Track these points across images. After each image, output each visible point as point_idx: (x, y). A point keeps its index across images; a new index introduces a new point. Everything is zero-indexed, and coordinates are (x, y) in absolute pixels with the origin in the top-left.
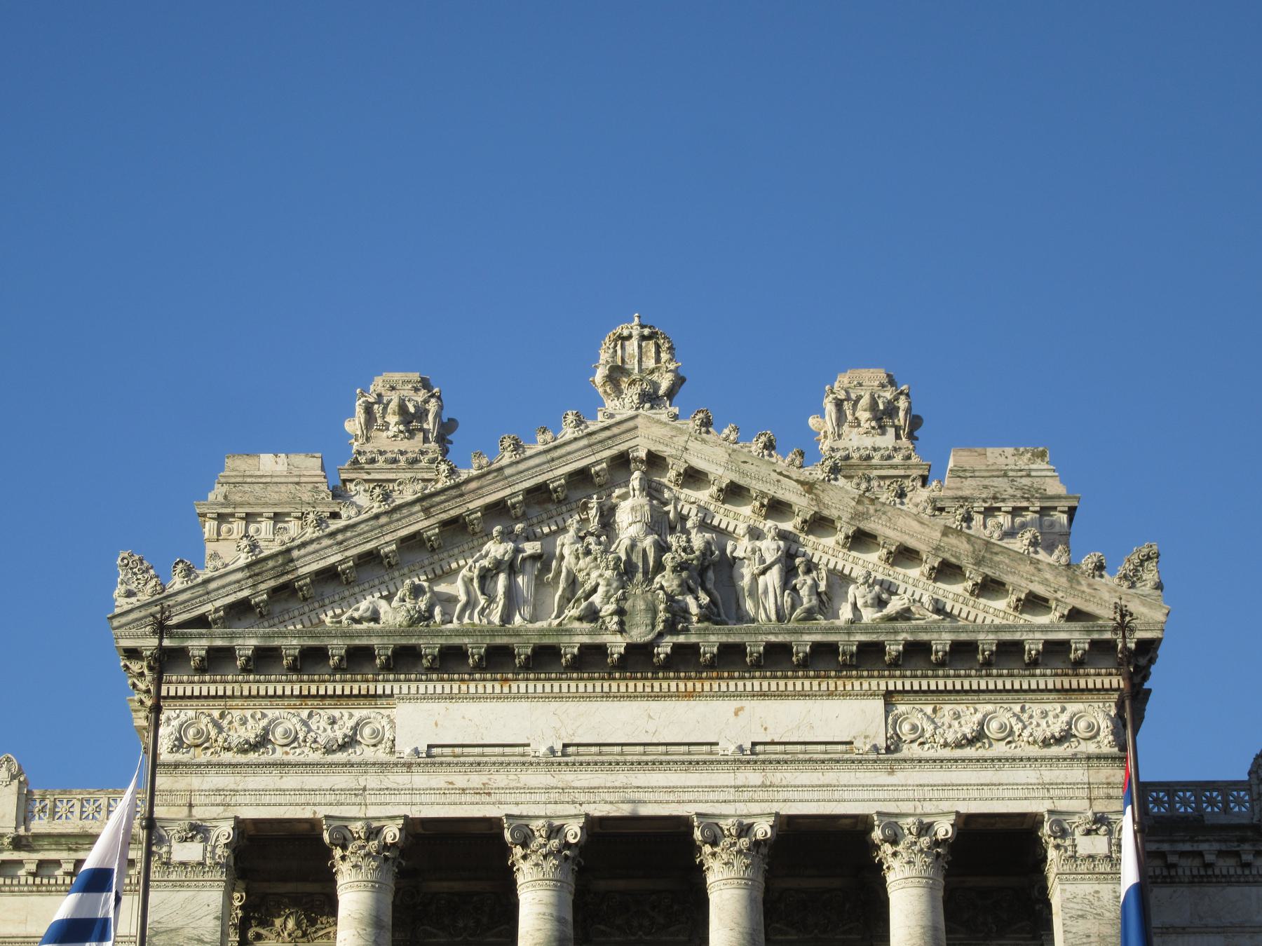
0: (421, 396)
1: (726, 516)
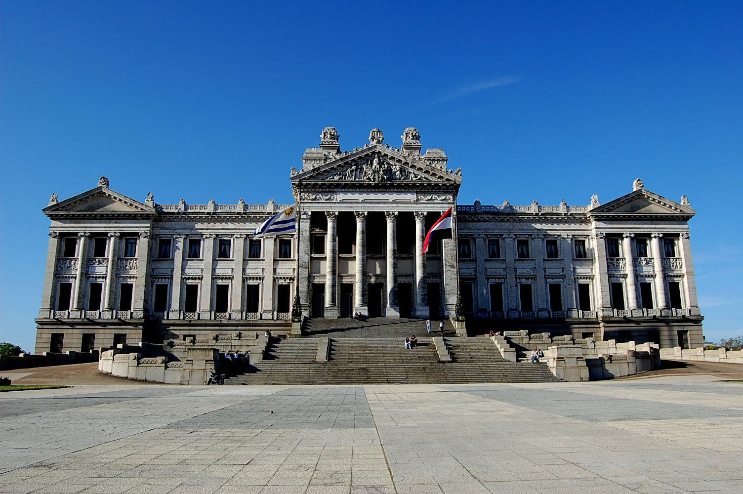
0: (334, 131)
1: (391, 162)
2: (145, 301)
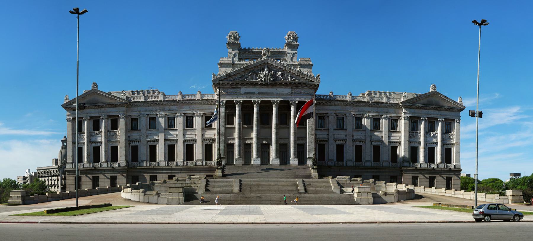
2: (126, 156)
